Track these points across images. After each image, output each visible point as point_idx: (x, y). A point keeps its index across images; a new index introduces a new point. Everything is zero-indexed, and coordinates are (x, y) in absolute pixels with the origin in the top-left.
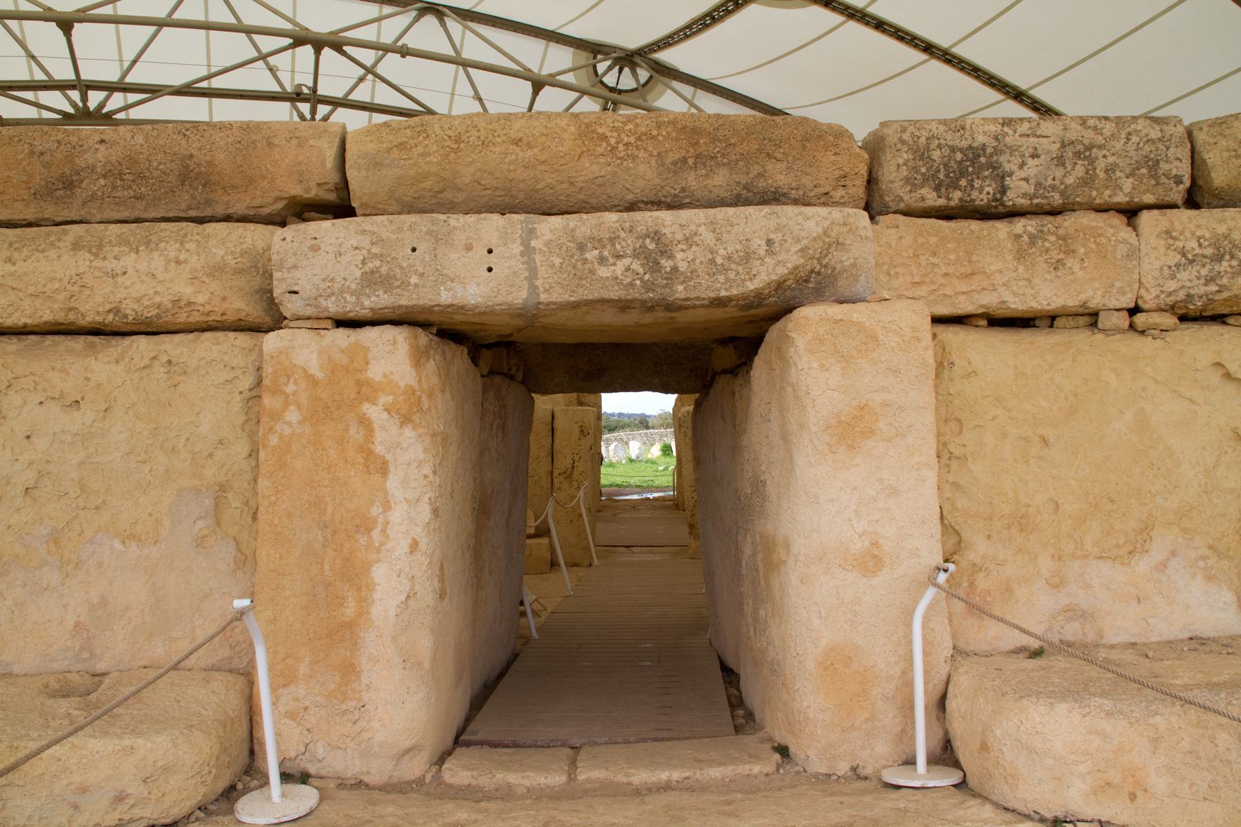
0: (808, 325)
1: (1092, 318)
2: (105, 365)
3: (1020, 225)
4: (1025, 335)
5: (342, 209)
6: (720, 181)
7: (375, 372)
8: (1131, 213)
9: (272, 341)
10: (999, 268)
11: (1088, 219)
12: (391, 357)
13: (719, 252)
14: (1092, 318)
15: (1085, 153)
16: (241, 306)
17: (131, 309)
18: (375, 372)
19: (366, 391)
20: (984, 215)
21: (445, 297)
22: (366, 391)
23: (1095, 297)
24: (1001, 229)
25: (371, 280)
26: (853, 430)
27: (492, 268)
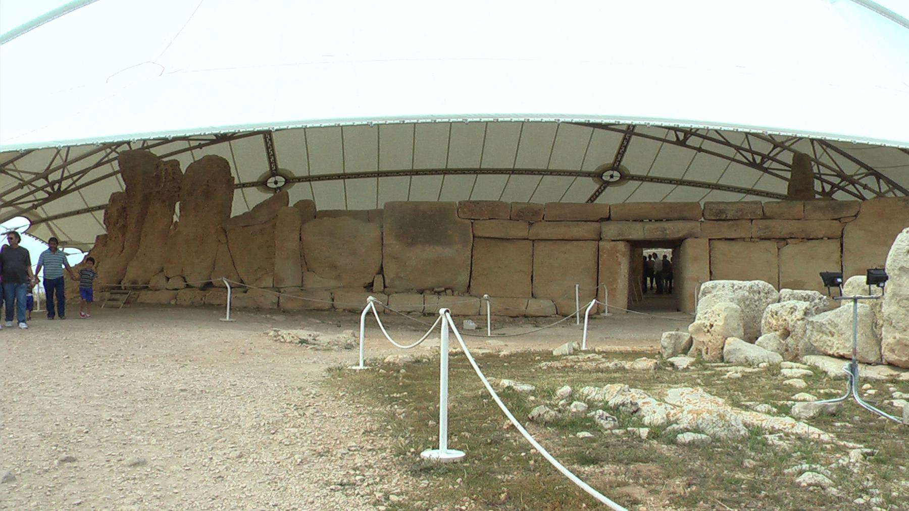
0: (689, 242)
1: (744, 239)
2: (568, 246)
3: (730, 222)
4: (733, 243)
5: (608, 219)
6: (676, 215)
7: (619, 248)
8: (752, 220)
9: (601, 243)
10: (726, 230)
11: (743, 221)
12: (621, 246)
13: (674, 229)
14: (744, 239)
15: (741, 210)
16: (594, 236)
17: (574, 238)
18: (619, 248)
19: (617, 252)
20: (724, 220)
21: (631, 237)
22: (617, 252)
23: (743, 235)
24: (726, 223)
25: (619, 235)
26: (695, 259)
27: (638, 232)
